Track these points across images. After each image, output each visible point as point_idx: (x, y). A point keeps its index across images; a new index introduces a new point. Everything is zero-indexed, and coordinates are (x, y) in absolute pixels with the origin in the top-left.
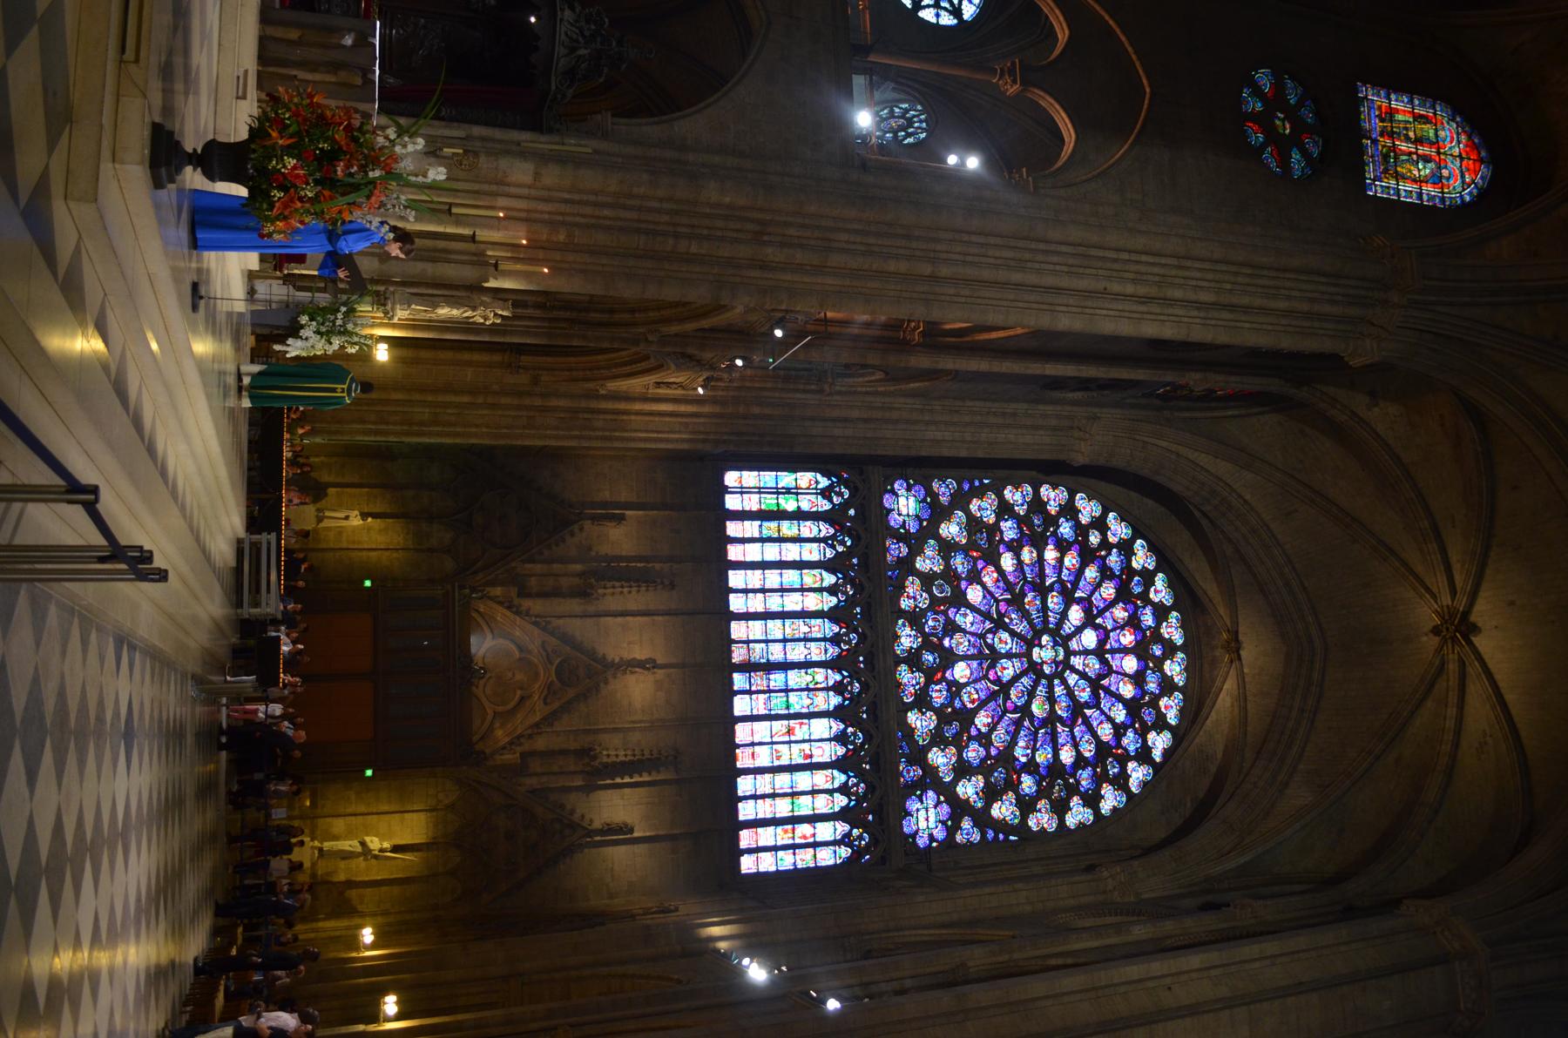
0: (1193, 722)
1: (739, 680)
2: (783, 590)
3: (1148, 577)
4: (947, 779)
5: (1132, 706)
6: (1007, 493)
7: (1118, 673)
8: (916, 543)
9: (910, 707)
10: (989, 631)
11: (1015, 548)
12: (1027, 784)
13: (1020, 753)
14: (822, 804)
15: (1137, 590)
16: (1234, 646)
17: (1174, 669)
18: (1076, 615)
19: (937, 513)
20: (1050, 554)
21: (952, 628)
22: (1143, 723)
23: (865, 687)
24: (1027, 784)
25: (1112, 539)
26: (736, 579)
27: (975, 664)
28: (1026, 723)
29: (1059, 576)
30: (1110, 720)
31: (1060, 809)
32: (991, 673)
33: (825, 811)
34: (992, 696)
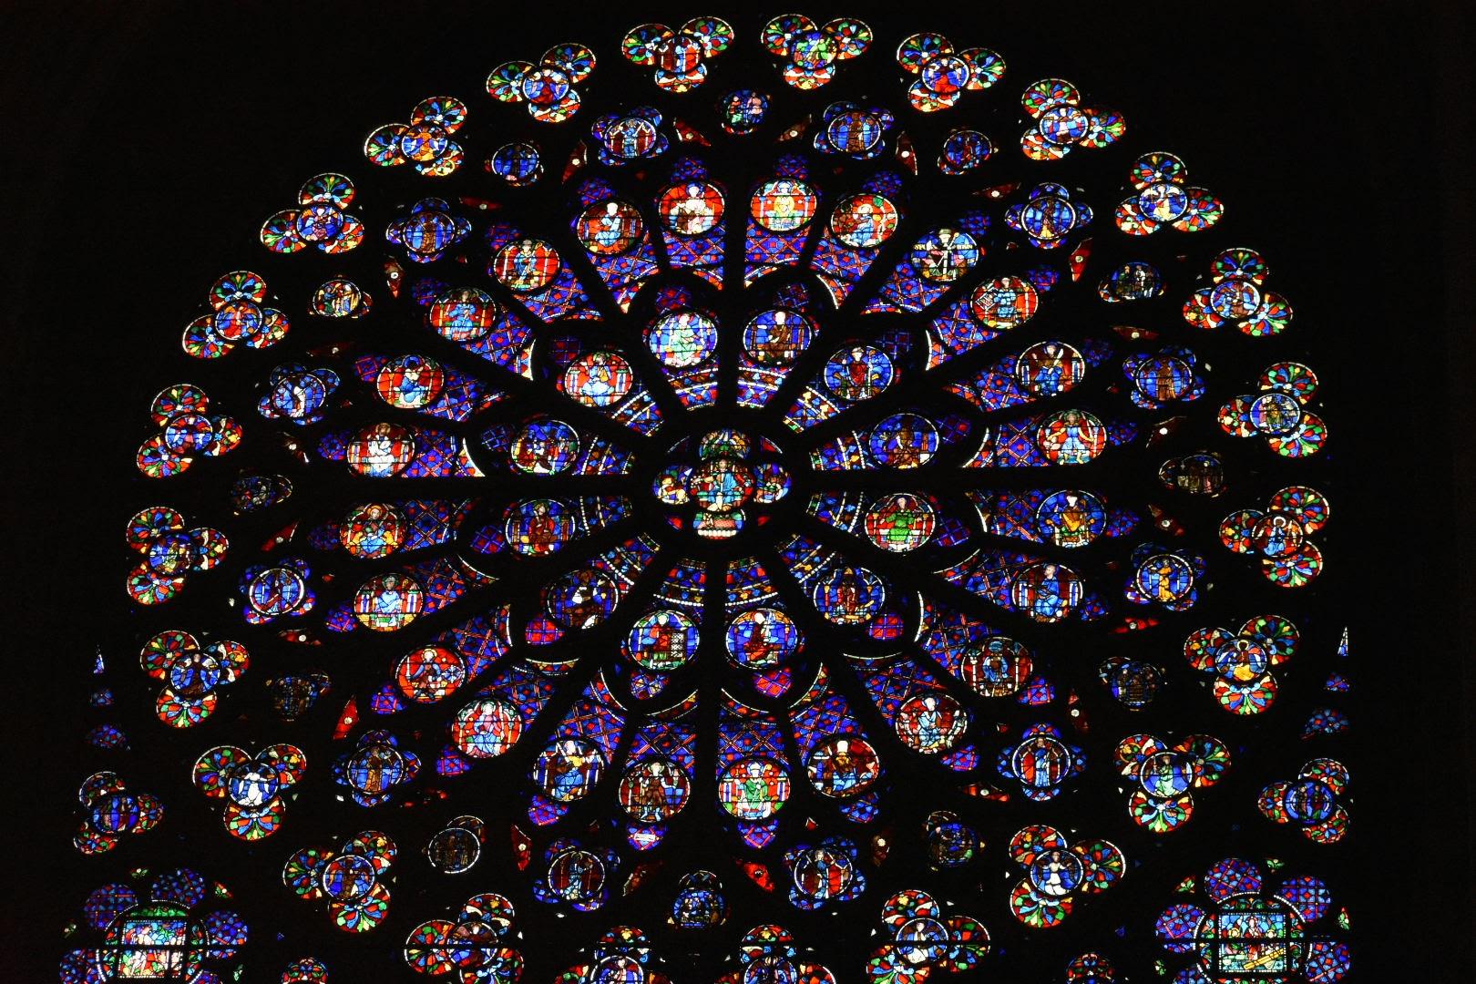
3: (495, 127)
4: (1120, 863)
7: (810, 249)
10: (620, 686)
11: (346, 578)
12: (1161, 583)
15: (532, 161)
17: (813, 60)
18: (595, 384)
24: (1161, 583)
27: (731, 744)
29: (457, 430)
30: (969, 282)
31: (1257, 474)
32: (766, 686)
34: (848, 689)
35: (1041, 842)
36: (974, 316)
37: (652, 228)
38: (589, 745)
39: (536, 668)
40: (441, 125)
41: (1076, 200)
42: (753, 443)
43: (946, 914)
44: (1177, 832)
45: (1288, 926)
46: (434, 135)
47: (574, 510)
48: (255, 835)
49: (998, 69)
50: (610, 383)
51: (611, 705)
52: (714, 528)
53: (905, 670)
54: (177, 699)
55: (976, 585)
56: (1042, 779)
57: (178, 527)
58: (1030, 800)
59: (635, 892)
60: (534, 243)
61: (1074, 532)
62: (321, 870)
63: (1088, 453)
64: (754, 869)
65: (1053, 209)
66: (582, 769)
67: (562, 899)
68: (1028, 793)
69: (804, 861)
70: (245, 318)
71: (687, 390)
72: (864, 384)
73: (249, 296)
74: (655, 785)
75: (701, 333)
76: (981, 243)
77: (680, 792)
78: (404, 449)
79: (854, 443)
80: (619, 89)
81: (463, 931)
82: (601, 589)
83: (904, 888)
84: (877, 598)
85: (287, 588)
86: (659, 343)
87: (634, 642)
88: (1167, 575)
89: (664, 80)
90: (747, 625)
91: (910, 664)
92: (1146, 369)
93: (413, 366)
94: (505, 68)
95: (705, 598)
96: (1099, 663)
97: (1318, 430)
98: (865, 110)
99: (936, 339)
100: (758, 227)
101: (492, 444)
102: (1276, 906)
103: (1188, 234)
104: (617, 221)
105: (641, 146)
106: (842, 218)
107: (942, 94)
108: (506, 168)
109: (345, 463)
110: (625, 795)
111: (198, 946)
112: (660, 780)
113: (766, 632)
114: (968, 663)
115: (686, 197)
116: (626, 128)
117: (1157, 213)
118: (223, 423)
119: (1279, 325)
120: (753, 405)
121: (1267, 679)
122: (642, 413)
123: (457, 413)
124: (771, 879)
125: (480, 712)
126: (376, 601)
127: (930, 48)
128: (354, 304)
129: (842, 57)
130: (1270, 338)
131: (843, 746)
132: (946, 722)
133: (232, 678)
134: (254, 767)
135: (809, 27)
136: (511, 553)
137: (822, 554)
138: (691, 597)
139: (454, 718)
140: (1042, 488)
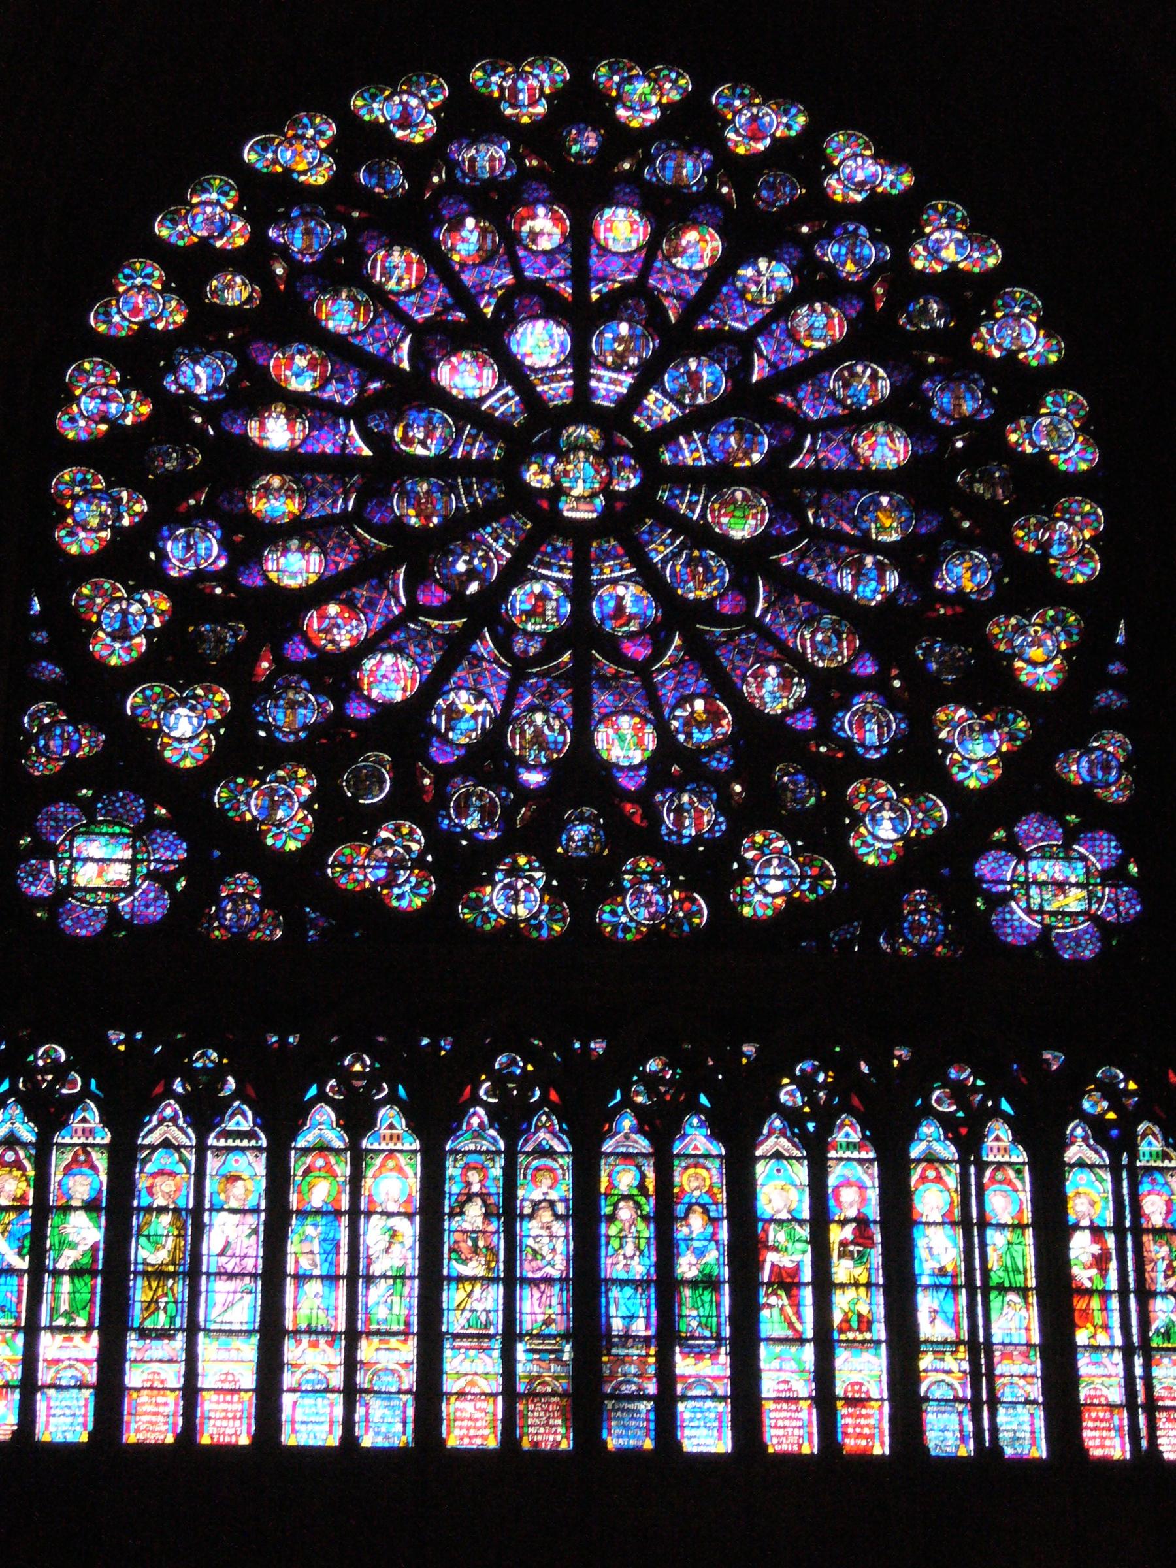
1: (627, 1433)
2: (356, 1277)
3: (359, 144)
4: (943, 813)
5: (746, 238)
7: (646, 270)
9: (724, 911)
11: (252, 539)
12: (963, 575)
13: (875, 587)
14: (1008, 1201)
15: (398, 179)
17: (643, 100)
18: (464, 377)
19: (129, 773)
24: (963, 575)
25: (238, 236)
26: (311, 1424)
27: (603, 699)
29: (347, 413)
30: (785, 307)
31: (1041, 486)
33: (1026, 1196)
34: (701, 654)
35: (873, 793)
36: (792, 335)
37: (508, 245)
38: (480, 696)
40: (313, 138)
41: (874, 238)
42: (606, 435)
44: (988, 790)
45: (1088, 873)
46: (307, 147)
47: (453, 488)
48: (188, 763)
49: (801, 120)
50: (479, 377)
51: (497, 661)
52: (577, 510)
54: (108, 640)
55: (807, 569)
56: (872, 738)
57: (99, 486)
58: (862, 756)
59: (528, 823)
60: (402, 251)
61: (888, 528)
62: (249, 795)
63: (895, 460)
64: (629, 808)
65: (854, 245)
66: (475, 716)
67: (464, 828)
68: (861, 750)
69: (672, 802)
70: (146, 301)
71: (546, 388)
72: (701, 390)
73: (149, 282)
74: (538, 733)
75: (556, 338)
76: (795, 272)
77: (561, 739)
78: (298, 426)
79: (694, 441)
80: (470, 116)
81: (378, 852)
82: (482, 559)
83: (762, 826)
84: (722, 578)
85: (202, 547)
86: (518, 344)
87: (513, 606)
88: (968, 569)
89: (509, 111)
90: (611, 596)
91: (753, 636)
94: (367, 90)
95: (573, 571)
96: (917, 641)
97: (1090, 450)
99: (761, 355)
100: (599, 246)
101: (377, 426)
102: (1075, 855)
103: (968, 274)
104: (476, 234)
105: (492, 169)
106: (674, 243)
107: (756, 137)
108: (374, 181)
109: (245, 437)
110: (513, 740)
111: (143, 861)
112: (545, 728)
113: (628, 602)
114: (802, 636)
115: (534, 217)
116: (477, 151)
117: (944, 254)
118: (134, 395)
119: (1053, 358)
120: (606, 404)
121: (1058, 661)
123: (345, 396)
124: (643, 818)
125: (380, 662)
126: (282, 560)
127: (741, 97)
128: (245, 295)
129: (664, 100)
130: (1045, 369)
131: (699, 704)
132: (787, 687)
133: (157, 623)
134: (183, 702)
135: (634, 72)
136: (400, 523)
137: (673, 537)
138: (561, 569)
139: (358, 667)
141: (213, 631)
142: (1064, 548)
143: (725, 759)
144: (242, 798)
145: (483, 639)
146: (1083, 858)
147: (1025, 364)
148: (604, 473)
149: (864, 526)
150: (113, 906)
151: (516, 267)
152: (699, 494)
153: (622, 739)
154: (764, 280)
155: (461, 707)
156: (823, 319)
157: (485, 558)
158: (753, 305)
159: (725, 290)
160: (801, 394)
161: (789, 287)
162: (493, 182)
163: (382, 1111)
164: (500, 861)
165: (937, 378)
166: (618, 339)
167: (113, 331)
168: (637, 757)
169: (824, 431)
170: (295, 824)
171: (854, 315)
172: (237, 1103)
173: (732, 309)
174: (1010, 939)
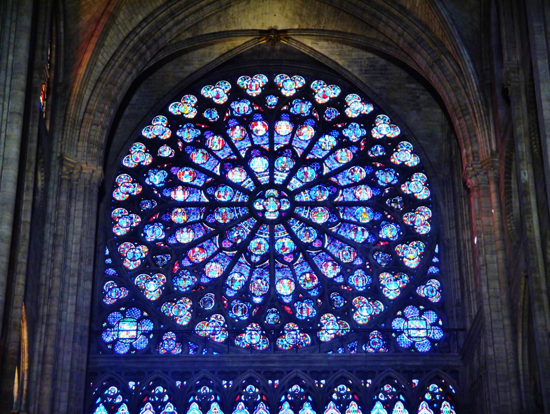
0: (339, 75)
3: (204, 104)
4: (382, 307)
5: (322, 129)
6: (120, 232)
7: (291, 140)
8: (165, 324)
9: (316, 340)
10: (248, 259)
11: (172, 229)
12: (389, 232)
13: (361, 237)
15: (215, 114)
16: (273, 34)
18: (236, 176)
20: (179, 195)
21: (245, 294)
22: (338, 120)
23: (296, 381)
24: (389, 232)
25: (167, 135)
27: (279, 275)
28: (334, 229)
31: (412, 203)
34: (308, 259)
36: (336, 159)
38: (242, 275)
39: (226, 254)
41: (361, 127)
42: (279, 193)
43: (337, 320)
47: (233, 211)
48: (154, 299)
50: (241, 176)
51: (246, 264)
53: (323, 255)
54: (129, 261)
55: (340, 232)
58: (357, 290)
59: (256, 314)
62: (172, 308)
66: (240, 281)
68: (357, 288)
71: (261, 178)
72: (307, 177)
73: (141, 150)
74: (259, 286)
75: (264, 163)
76: (337, 139)
77: (266, 287)
78: (186, 193)
92: (382, 174)
93: (187, 170)
95: (269, 235)
96: (373, 254)
97: (427, 191)
98: (303, 102)
99: (326, 165)
102: (422, 319)
104: (240, 131)
105: (244, 111)
109: (170, 197)
110: (251, 288)
115: (257, 125)
119: (416, 163)
120: (279, 183)
121: (417, 258)
122: (249, 185)
124: (291, 310)
125: (211, 266)
128: (170, 153)
129: (297, 87)
132: (335, 269)
133: (144, 256)
134: (152, 280)
136: (216, 221)
137: (300, 223)
138: (266, 234)
139: (204, 267)
140: (356, 206)
141: (161, 258)
142: (420, 223)
143: (316, 292)
144: (170, 309)
145: (242, 257)
146: (425, 320)
147: (407, 166)
148: (279, 204)
149: (358, 218)
150: (131, 343)
151: (251, 140)
152: (307, 209)
153: (284, 287)
154: (327, 142)
155: (236, 279)
156: (344, 154)
157: (243, 232)
158: (324, 150)
159: (315, 146)
160: (338, 178)
161: (335, 144)
162: (244, 115)
163: (212, 405)
164: (248, 326)
165: (380, 171)
166: (283, 162)
167: (130, 166)
168: (289, 292)
169: (346, 188)
170: (185, 316)
171: (355, 152)
172: (169, 403)
173: (318, 151)
174: (403, 345)
